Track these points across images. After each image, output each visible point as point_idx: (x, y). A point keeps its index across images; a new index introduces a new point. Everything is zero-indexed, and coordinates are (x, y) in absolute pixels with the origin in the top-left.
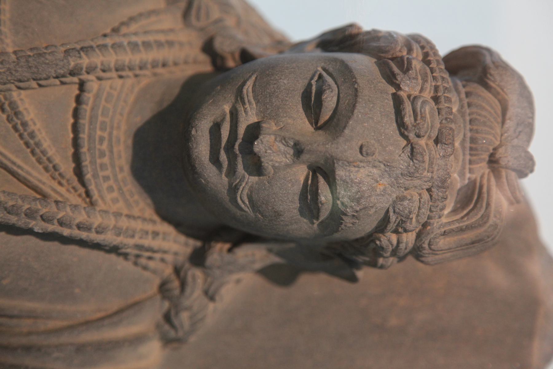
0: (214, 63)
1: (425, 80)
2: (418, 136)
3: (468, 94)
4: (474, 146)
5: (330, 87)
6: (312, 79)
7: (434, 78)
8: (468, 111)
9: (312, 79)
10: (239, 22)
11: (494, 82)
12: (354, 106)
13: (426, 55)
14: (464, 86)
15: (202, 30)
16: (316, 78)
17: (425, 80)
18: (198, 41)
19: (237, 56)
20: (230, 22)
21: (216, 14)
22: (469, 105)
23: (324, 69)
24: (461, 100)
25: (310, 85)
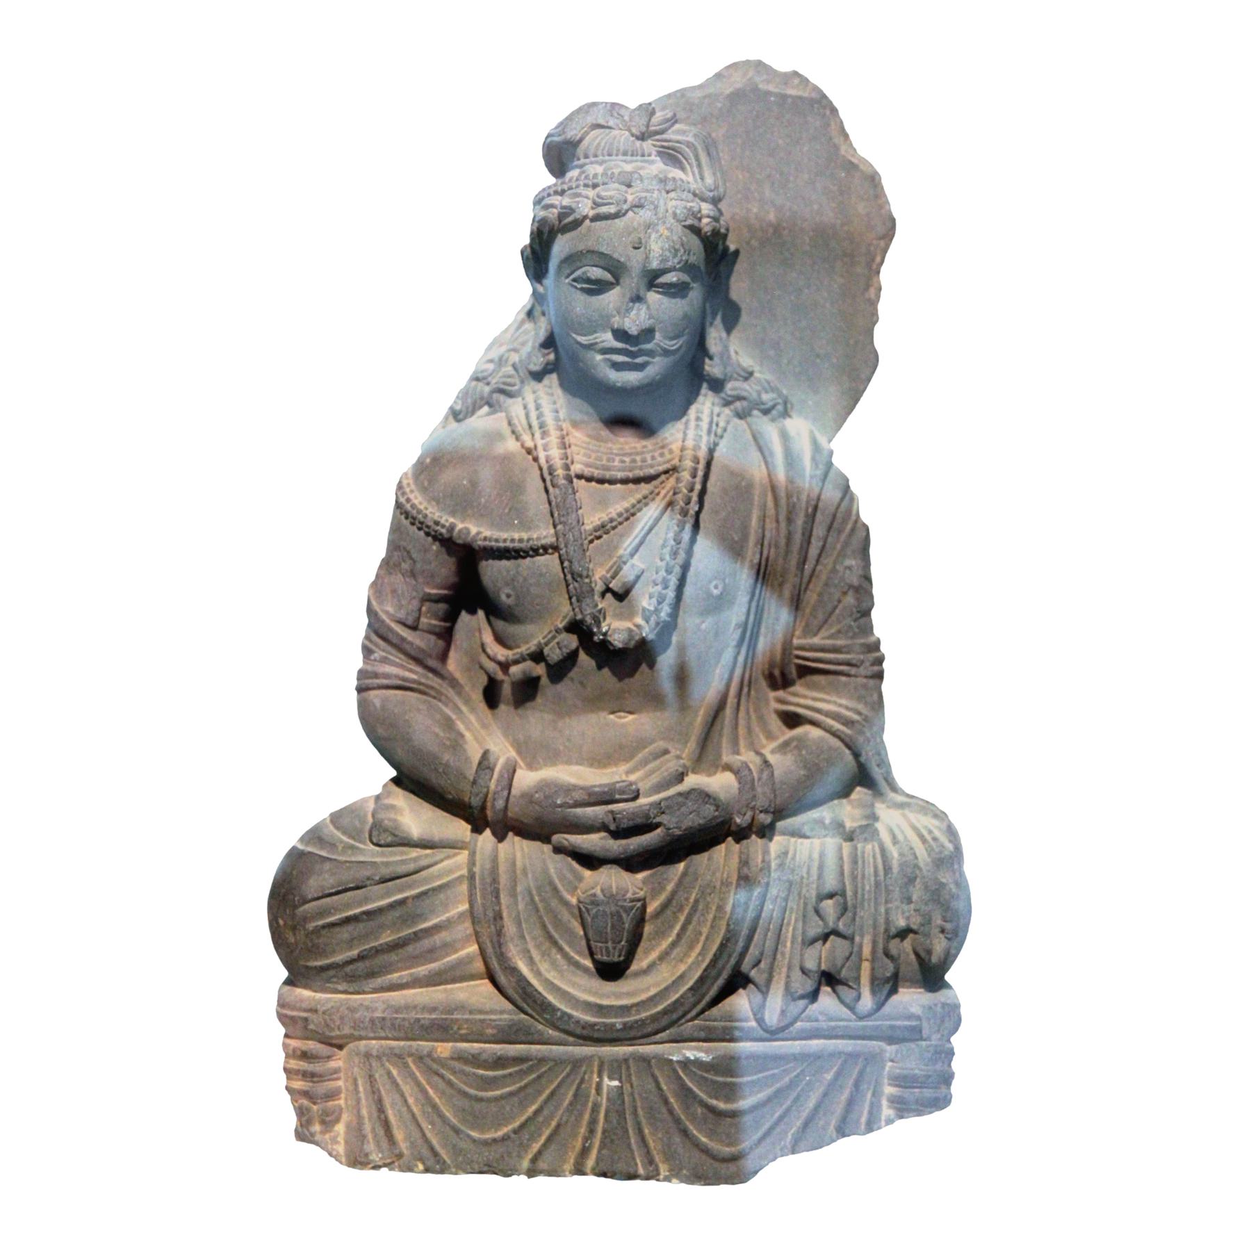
0: (551, 372)
1: (579, 195)
2: (625, 201)
3: (586, 157)
4: (630, 153)
5: (584, 273)
6: (576, 287)
7: (577, 187)
8: (601, 157)
9: (576, 287)
10: (515, 350)
11: (576, 135)
12: (602, 253)
13: (556, 193)
14: (579, 159)
15: (522, 382)
16: (575, 284)
17: (579, 195)
18: (533, 384)
19: (546, 351)
20: (515, 358)
21: (508, 369)
22: (596, 156)
23: (567, 277)
24: (592, 163)
25: (582, 289)
